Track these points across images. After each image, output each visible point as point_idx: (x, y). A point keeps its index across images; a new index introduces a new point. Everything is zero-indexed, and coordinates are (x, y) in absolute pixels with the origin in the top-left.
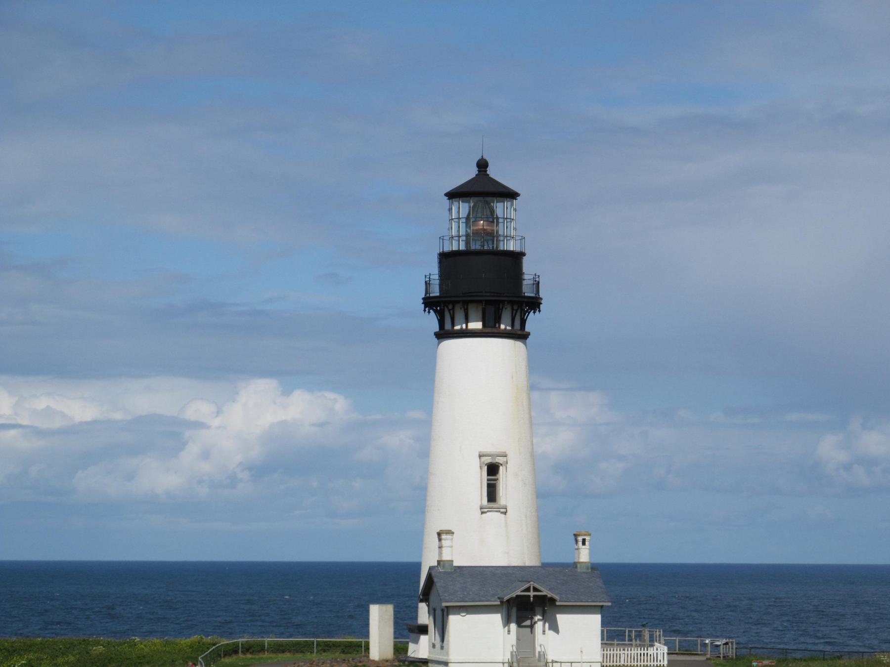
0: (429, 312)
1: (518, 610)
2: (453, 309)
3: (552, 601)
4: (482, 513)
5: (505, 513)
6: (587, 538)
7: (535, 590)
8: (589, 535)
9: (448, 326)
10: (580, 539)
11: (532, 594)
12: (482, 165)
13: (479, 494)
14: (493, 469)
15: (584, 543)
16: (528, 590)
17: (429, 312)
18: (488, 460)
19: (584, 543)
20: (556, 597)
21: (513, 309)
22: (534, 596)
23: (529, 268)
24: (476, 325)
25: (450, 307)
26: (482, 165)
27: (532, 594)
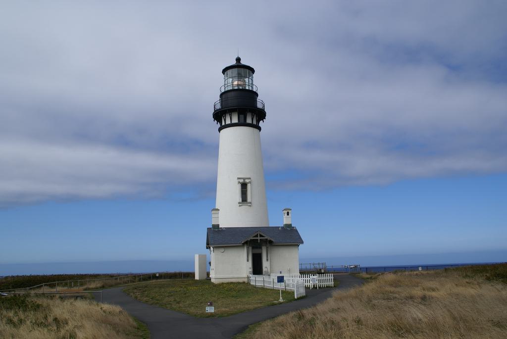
1: (253, 248)
3: (271, 242)
4: (240, 206)
5: (250, 206)
7: (261, 236)
9: (223, 124)
10: (286, 212)
11: (259, 238)
12: (238, 60)
13: (239, 198)
14: (244, 186)
15: (288, 214)
16: (257, 236)
18: (242, 181)
19: (288, 214)
20: (272, 240)
21: (252, 115)
22: (260, 239)
23: (259, 98)
24: (235, 120)
25: (224, 115)
26: (238, 60)
27: (259, 238)
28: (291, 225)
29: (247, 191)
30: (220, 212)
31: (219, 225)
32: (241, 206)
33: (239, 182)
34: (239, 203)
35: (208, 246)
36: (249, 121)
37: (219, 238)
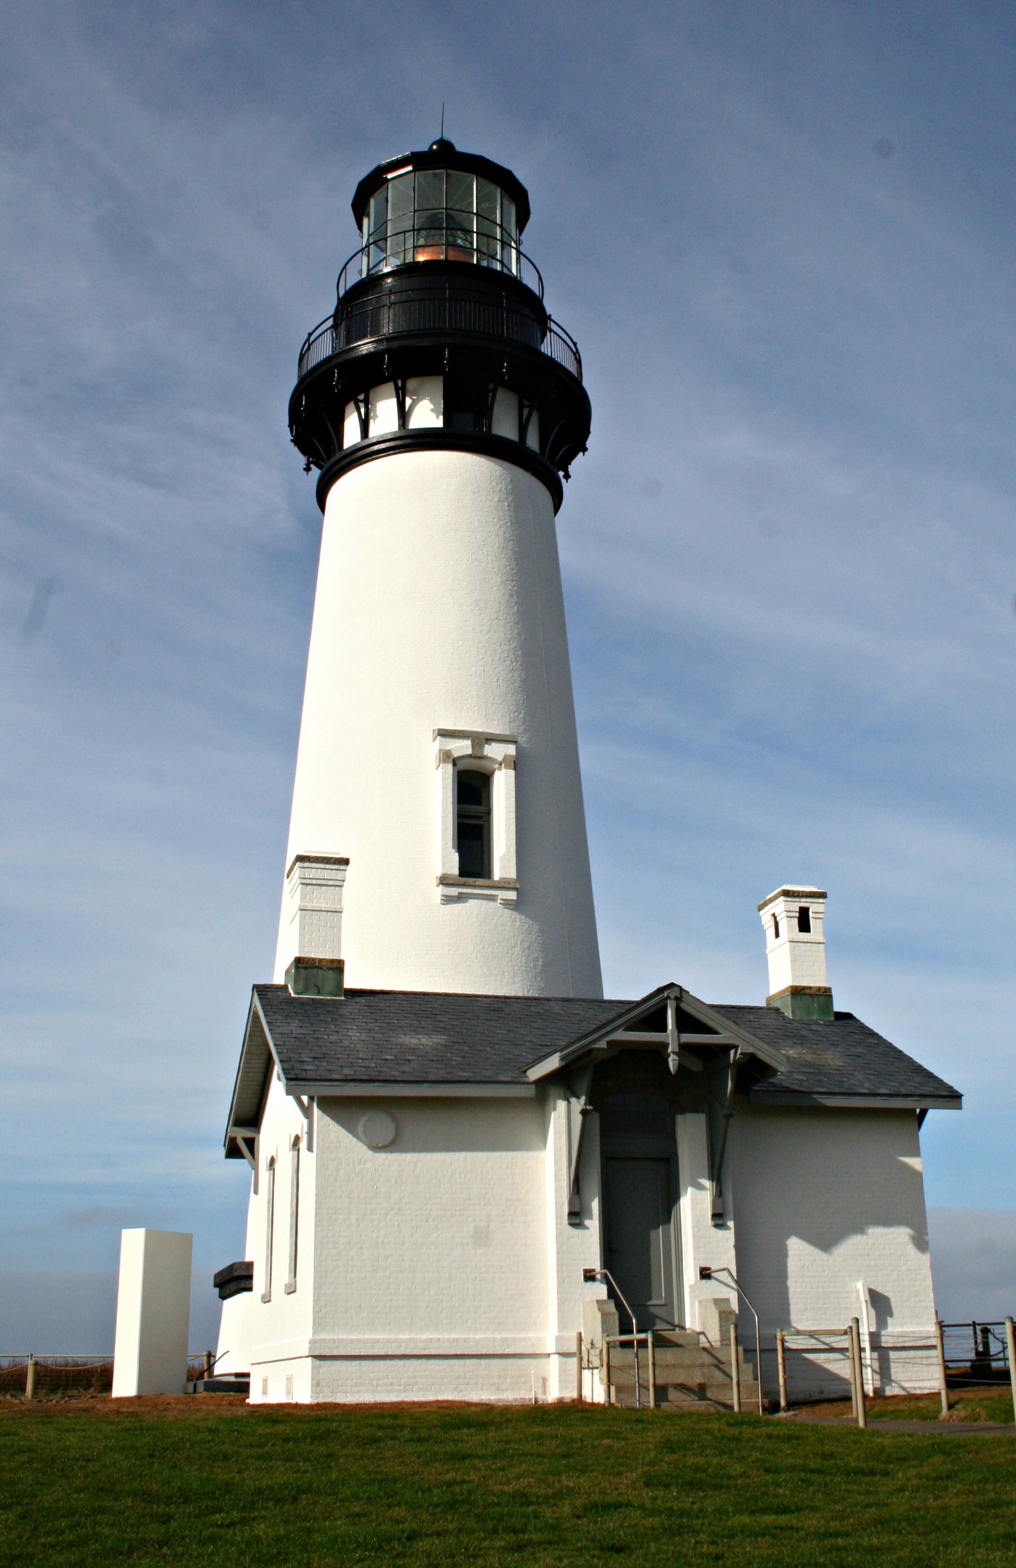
0: (308, 469)
2: (367, 402)
4: (448, 900)
6: (815, 907)
7: (687, 1022)
8: (822, 895)
15: (804, 925)
17: (308, 469)
19: (804, 925)
22: (685, 1048)
25: (361, 397)
28: (826, 994)
29: (489, 812)
30: (349, 868)
31: (337, 967)
32: (461, 898)
33: (446, 756)
34: (444, 881)
35: (241, 1134)
36: (504, 425)
37: (344, 1051)
